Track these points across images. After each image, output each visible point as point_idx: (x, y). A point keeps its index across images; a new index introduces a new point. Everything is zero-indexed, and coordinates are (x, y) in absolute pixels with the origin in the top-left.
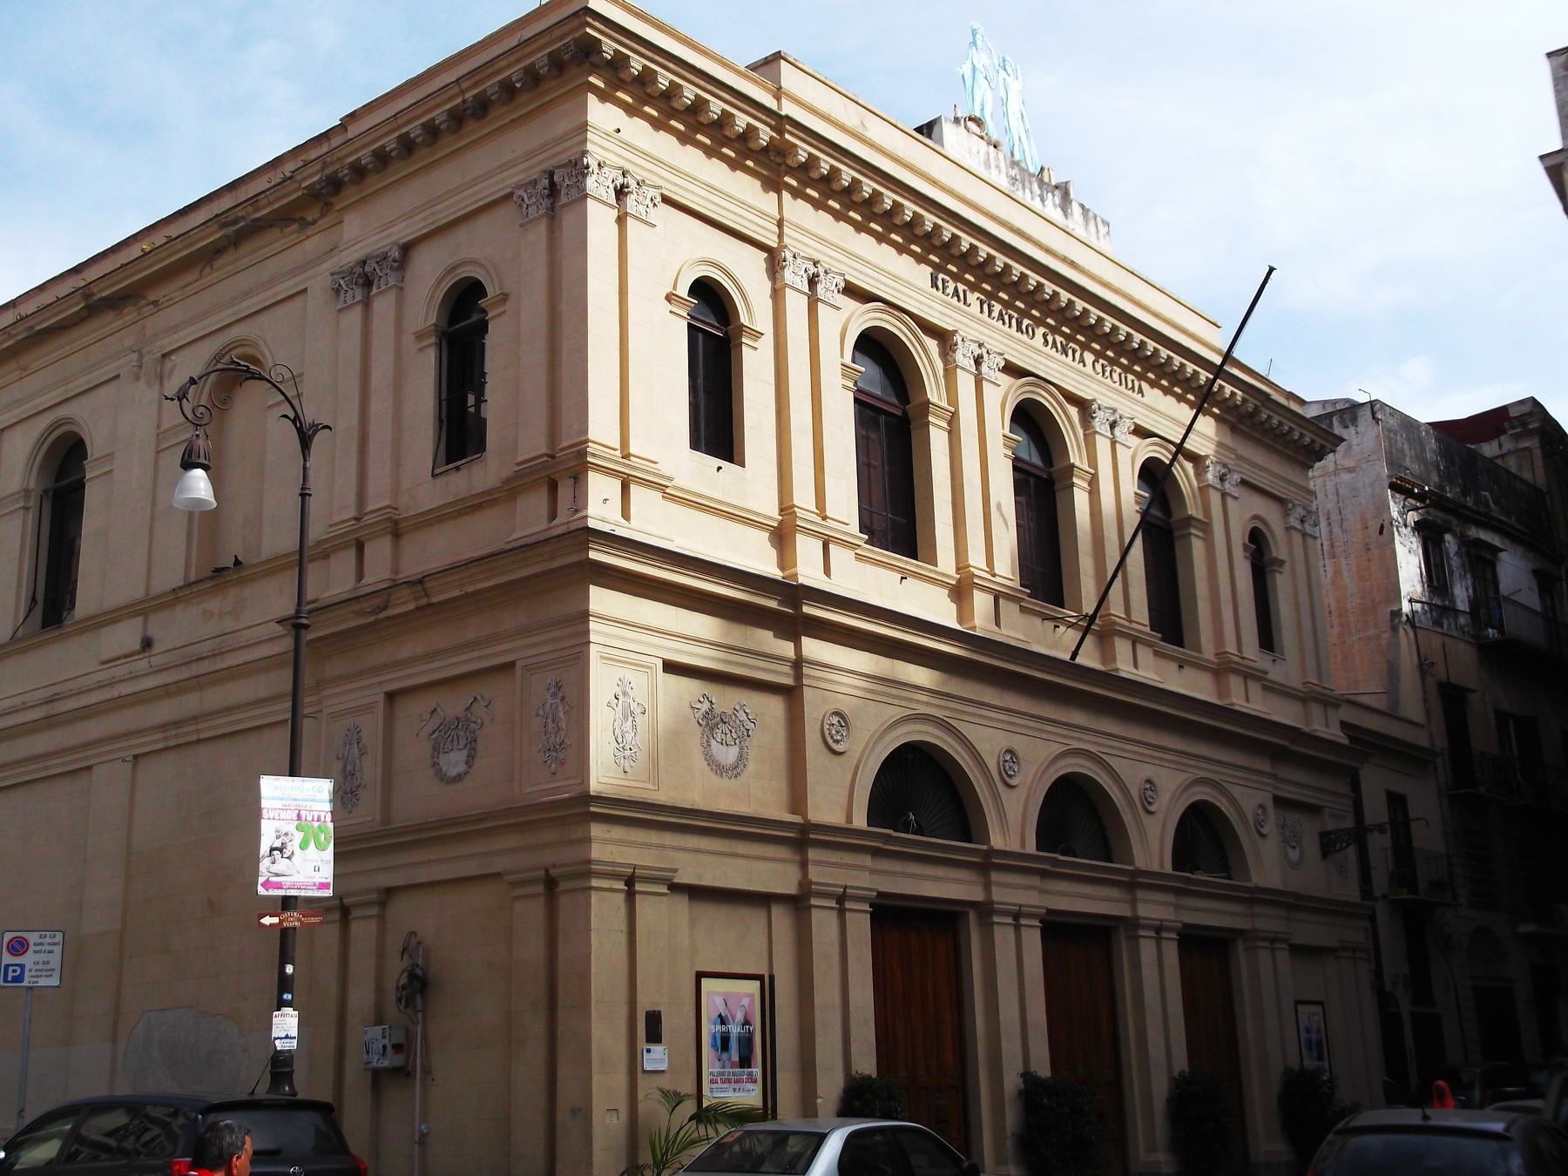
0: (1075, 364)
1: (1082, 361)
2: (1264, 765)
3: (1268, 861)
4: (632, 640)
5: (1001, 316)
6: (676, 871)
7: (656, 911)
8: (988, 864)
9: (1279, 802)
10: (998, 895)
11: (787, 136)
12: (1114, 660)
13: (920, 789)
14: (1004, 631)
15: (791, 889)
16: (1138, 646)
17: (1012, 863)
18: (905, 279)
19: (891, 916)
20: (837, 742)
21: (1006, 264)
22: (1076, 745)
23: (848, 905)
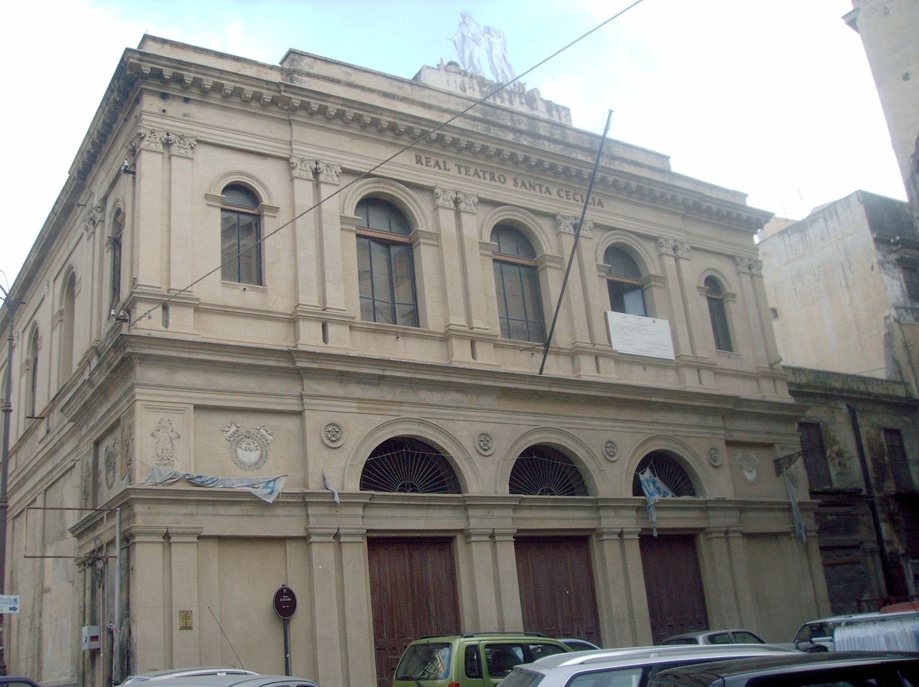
0: (543, 195)
1: (548, 190)
2: (719, 422)
3: (717, 484)
4: (185, 397)
5: (476, 173)
6: (201, 528)
7: (185, 555)
8: (598, 506)
9: (730, 443)
10: (473, 523)
11: (283, 93)
12: (580, 370)
13: (407, 464)
14: (602, 375)
15: (301, 533)
16: (601, 361)
17: (488, 503)
18: (368, 155)
19: (527, 543)
20: (486, 450)
21: (525, 157)
22: (542, 425)
23: (497, 538)
